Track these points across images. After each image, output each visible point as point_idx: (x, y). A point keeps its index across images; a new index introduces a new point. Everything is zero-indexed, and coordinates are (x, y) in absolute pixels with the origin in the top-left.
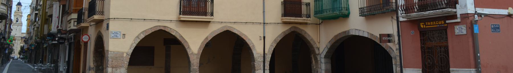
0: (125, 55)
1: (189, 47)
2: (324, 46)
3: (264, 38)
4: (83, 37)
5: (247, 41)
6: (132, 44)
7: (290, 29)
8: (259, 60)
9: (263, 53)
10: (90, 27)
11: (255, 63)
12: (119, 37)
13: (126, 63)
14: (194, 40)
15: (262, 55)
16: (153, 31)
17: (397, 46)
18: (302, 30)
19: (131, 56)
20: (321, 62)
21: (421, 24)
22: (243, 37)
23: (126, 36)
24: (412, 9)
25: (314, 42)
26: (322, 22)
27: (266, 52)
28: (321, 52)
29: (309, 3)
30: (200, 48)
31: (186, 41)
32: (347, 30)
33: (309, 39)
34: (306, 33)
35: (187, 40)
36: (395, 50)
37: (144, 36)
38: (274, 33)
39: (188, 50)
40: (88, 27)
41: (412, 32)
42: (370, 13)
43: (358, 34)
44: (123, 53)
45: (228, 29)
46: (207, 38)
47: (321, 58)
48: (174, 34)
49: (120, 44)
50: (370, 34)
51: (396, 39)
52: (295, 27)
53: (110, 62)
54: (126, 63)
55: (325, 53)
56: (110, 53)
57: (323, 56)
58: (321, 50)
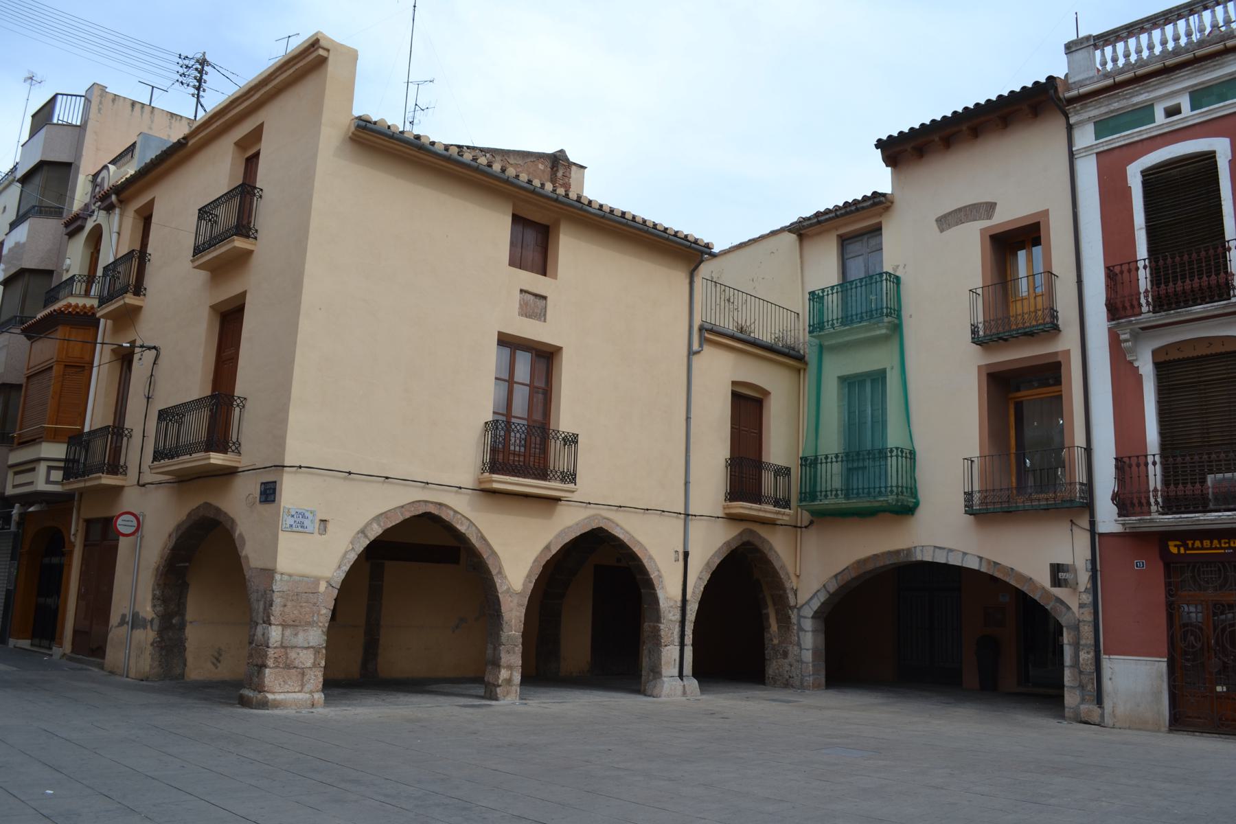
0: (323, 586)
1: (500, 572)
2: (816, 586)
3: (686, 554)
4: (119, 522)
5: (645, 561)
6: (346, 553)
7: (741, 534)
8: (671, 617)
9: (679, 598)
10: (127, 492)
11: (662, 627)
12: (310, 529)
13: (324, 611)
14: (517, 551)
15: (679, 604)
16: (408, 515)
17: (1087, 598)
18: (764, 540)
19: (340, 590)
20: (801, 629)
21: (1171, 544)
22: (635, 549)
23: (330, 526)
24: (1141, 504)
25: (787, 574)
26: (811, 523)
27: (688, 597)
28: (801, 601)
29: (788, 469)
30: (528, 576)
31: (494, 553)
32: (904, 547)
33: (777, 565)
34: (771, 548)
35: (496, 548)
36: (1074, 606)
37: (380, 531)
38: (709, 544)
39: (498, 581)
40: (122, 487)
41: (1140, 564)
42: (987, 509)
43: (943, 561)
44: (317, 580)
45: (601, 525)
46: (547, 548)
47: (800, 617)
48: (462, 528)
49: (309, 549)
50: (989, 562)
51: (1084, 578)
52: (751, 531)
53: (276, 609)
54: (324, 611)
55: (816, 604)
56: (278, 577)
57: (808, 612)
58: (803, 597)
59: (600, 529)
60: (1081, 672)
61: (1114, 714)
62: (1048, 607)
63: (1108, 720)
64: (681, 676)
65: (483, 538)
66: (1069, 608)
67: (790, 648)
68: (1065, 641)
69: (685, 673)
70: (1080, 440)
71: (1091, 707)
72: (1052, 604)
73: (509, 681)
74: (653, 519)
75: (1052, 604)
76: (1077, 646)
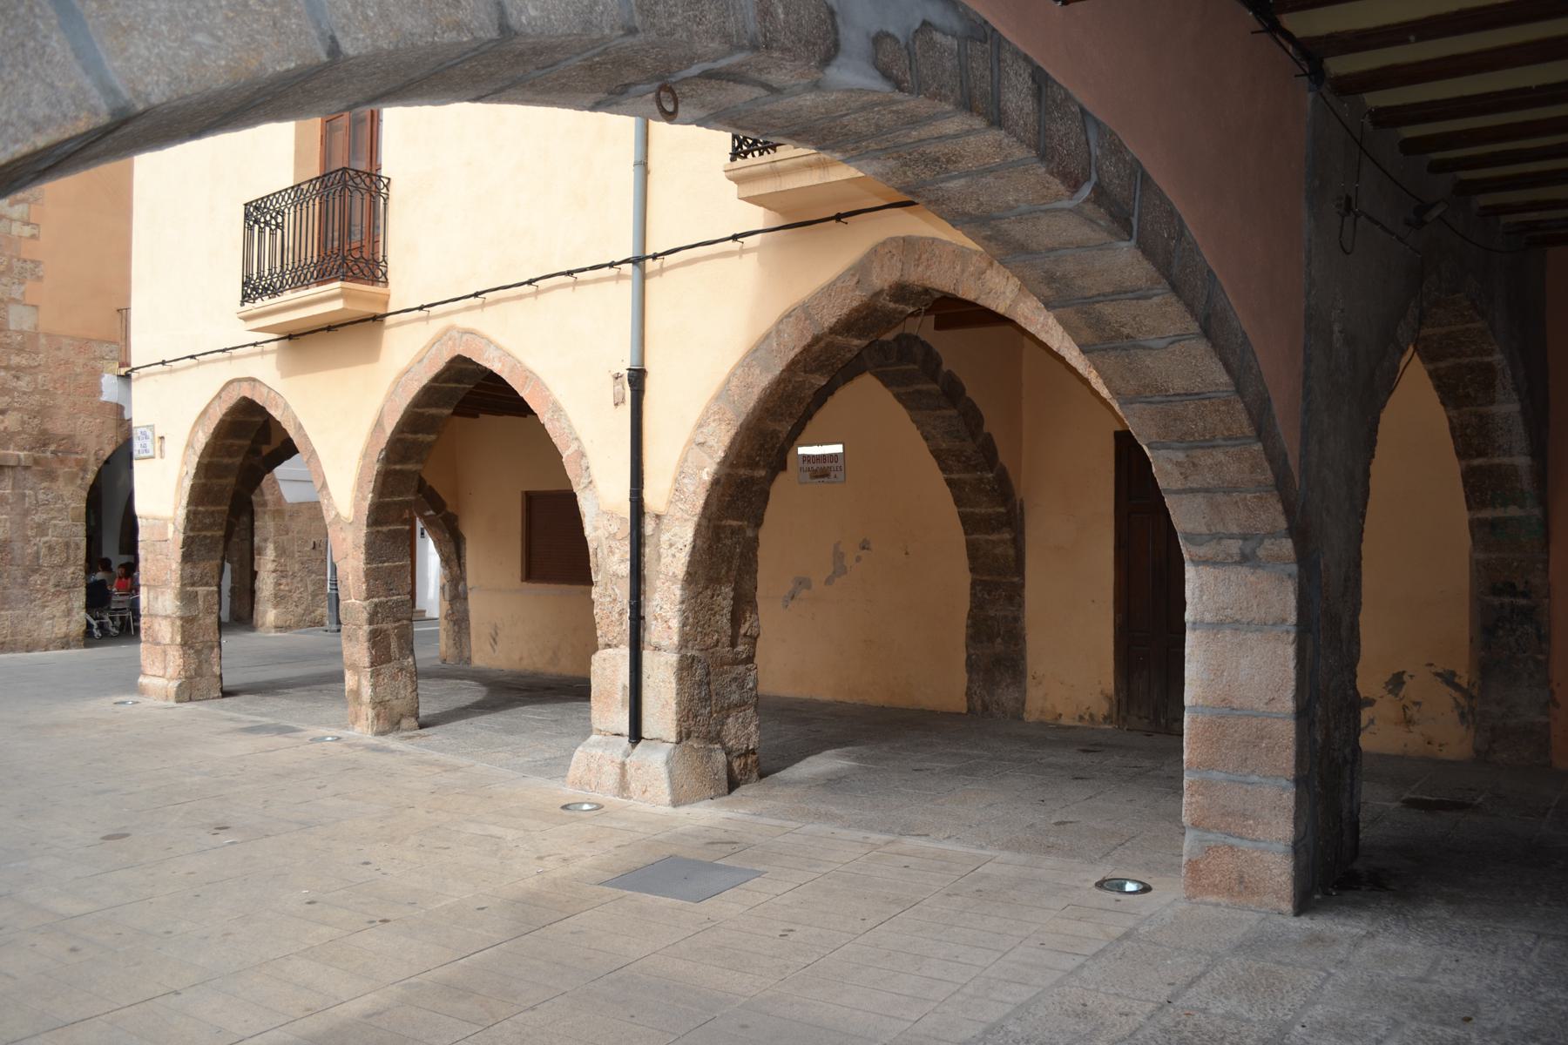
3: (637, 378)
7: (860, 270)
46: (379, 424)
52: (908, 244)
59: (459, 357)
64: (636, 735)
65: (300, 427)
69: (649, 727)
73: (357, 693)
74: (560, 299)
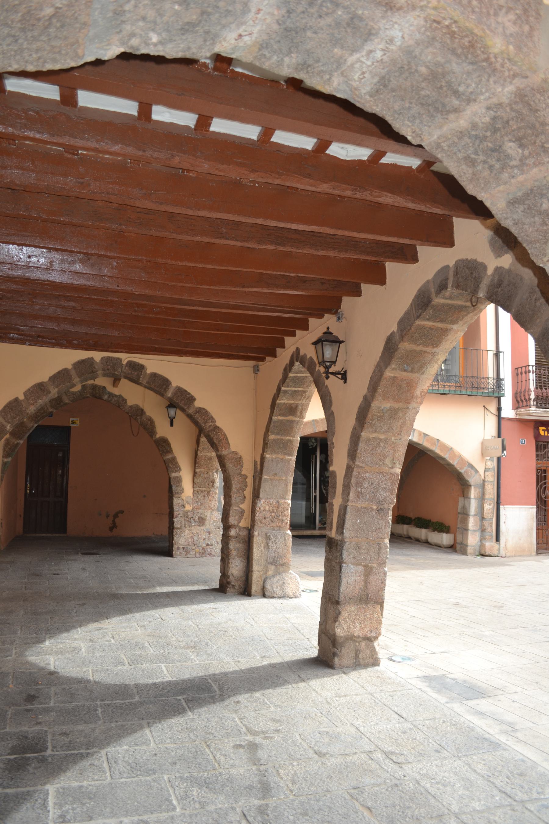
24: (526, 400)
36: (481, 471)
60: (483, 518)
61: (506, 548)
62: (462, 471)
63: (503, 553)
66: (477, 471)
67: (208, 514)
68: (472, 496)
70: (491, 345)
71: (492, 544)
72: (465, 468)
75: (465, 468)
76: (482, 499)
